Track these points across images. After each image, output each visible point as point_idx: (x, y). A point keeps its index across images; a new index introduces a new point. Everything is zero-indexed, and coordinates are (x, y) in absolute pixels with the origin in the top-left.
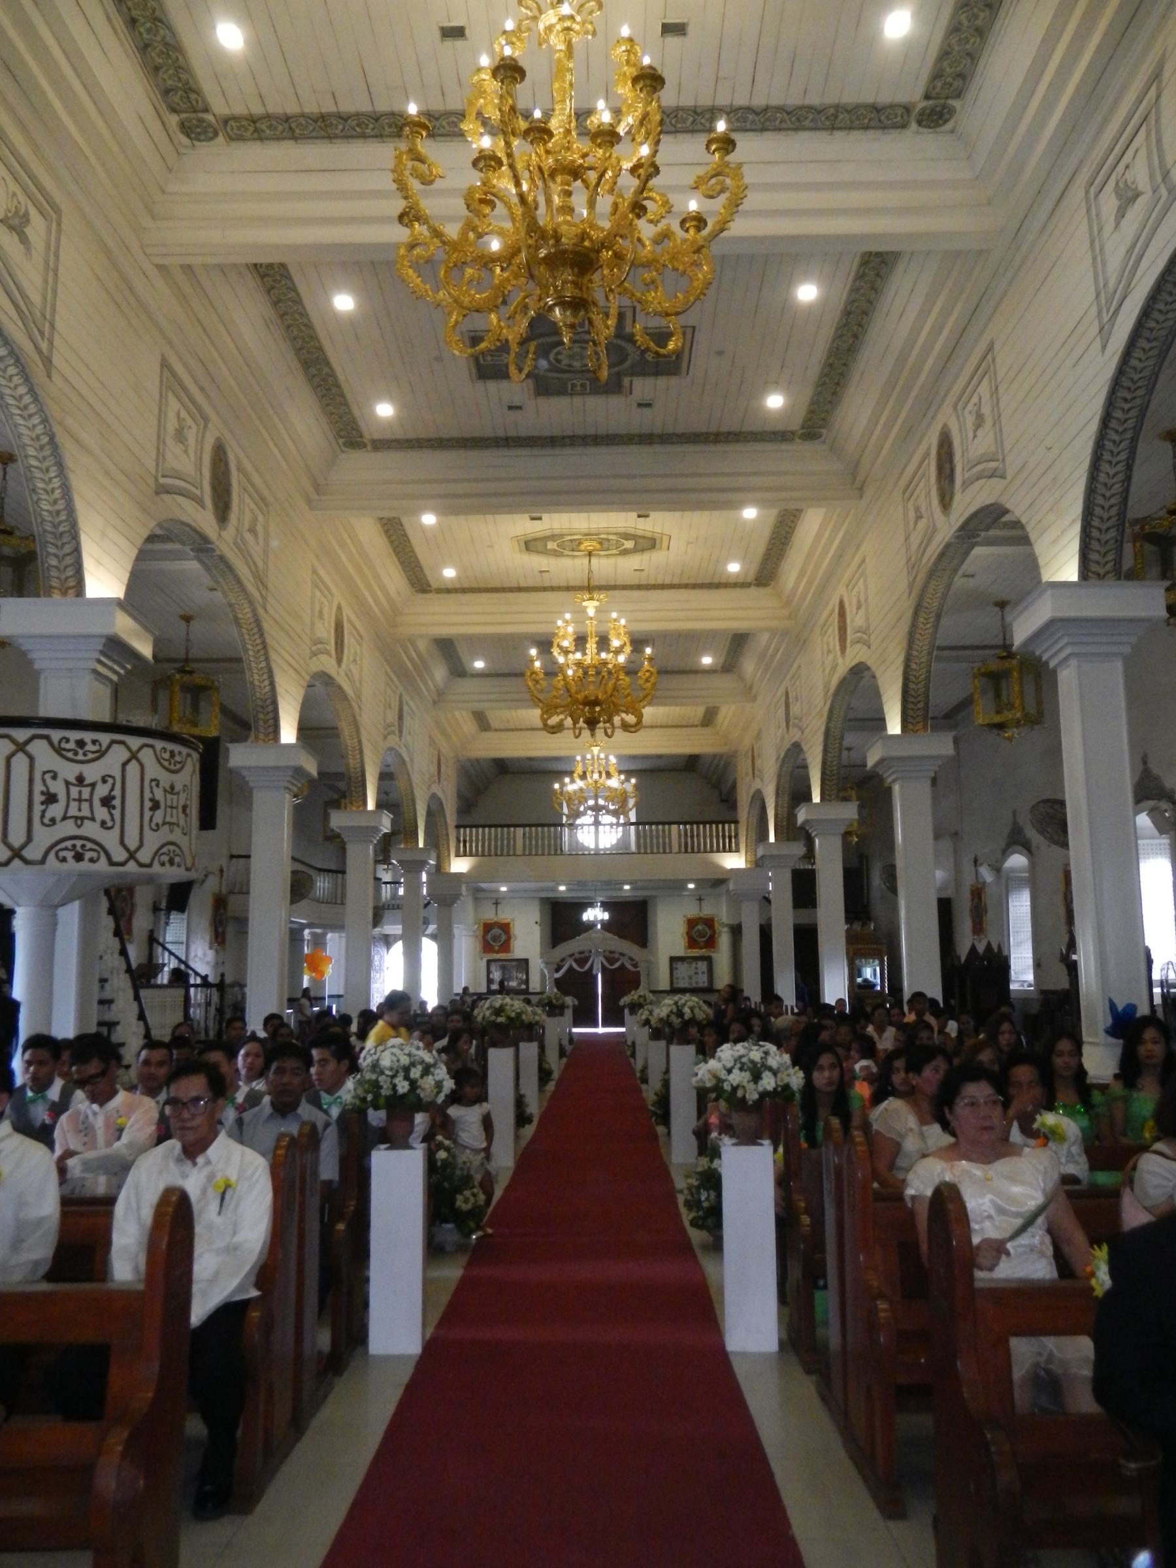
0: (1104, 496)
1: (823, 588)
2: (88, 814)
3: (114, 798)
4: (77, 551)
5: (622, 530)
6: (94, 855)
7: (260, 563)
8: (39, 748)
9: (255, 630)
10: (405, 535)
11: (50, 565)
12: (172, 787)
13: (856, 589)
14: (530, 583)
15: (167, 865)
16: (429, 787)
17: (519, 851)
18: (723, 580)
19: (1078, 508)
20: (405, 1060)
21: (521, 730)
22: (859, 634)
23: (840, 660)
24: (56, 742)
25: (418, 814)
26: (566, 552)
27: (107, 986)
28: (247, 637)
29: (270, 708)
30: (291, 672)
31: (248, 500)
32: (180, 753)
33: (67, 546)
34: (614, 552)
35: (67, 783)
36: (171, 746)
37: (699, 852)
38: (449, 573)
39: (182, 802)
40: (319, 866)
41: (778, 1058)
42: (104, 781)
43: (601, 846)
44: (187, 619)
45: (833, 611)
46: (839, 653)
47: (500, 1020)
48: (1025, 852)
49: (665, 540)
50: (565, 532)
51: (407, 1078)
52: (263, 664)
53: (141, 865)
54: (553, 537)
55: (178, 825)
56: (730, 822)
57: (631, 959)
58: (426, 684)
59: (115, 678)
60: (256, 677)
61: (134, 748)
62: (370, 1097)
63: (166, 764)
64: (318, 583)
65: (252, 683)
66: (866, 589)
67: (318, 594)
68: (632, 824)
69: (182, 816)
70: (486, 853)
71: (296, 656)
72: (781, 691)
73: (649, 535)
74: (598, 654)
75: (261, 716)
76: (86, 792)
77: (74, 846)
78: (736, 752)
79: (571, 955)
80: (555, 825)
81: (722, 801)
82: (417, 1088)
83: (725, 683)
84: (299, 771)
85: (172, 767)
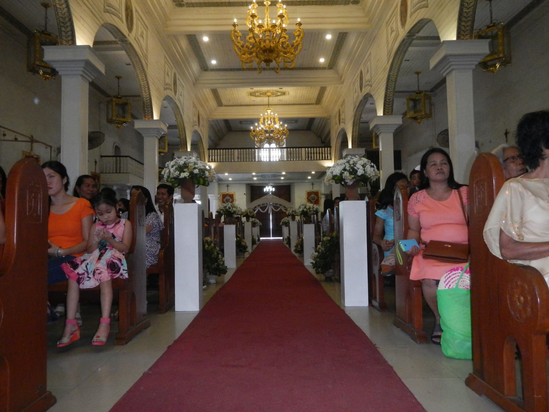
16: (193, 126)
21: (236, 106)
25: (187, 136)
29: (68, 24)
37: (314, 160)
45: (397, 6)
47: (183, 175)
56: (327, 147)
57: (284, 207)
58: (188, 70)
70: (222, 161)
72: (359, 72)
75: (63, 29)
78: (330, 116)
79: (259, 206)
80: (252, 148)
83: (329, 74)
84: (88, 64)
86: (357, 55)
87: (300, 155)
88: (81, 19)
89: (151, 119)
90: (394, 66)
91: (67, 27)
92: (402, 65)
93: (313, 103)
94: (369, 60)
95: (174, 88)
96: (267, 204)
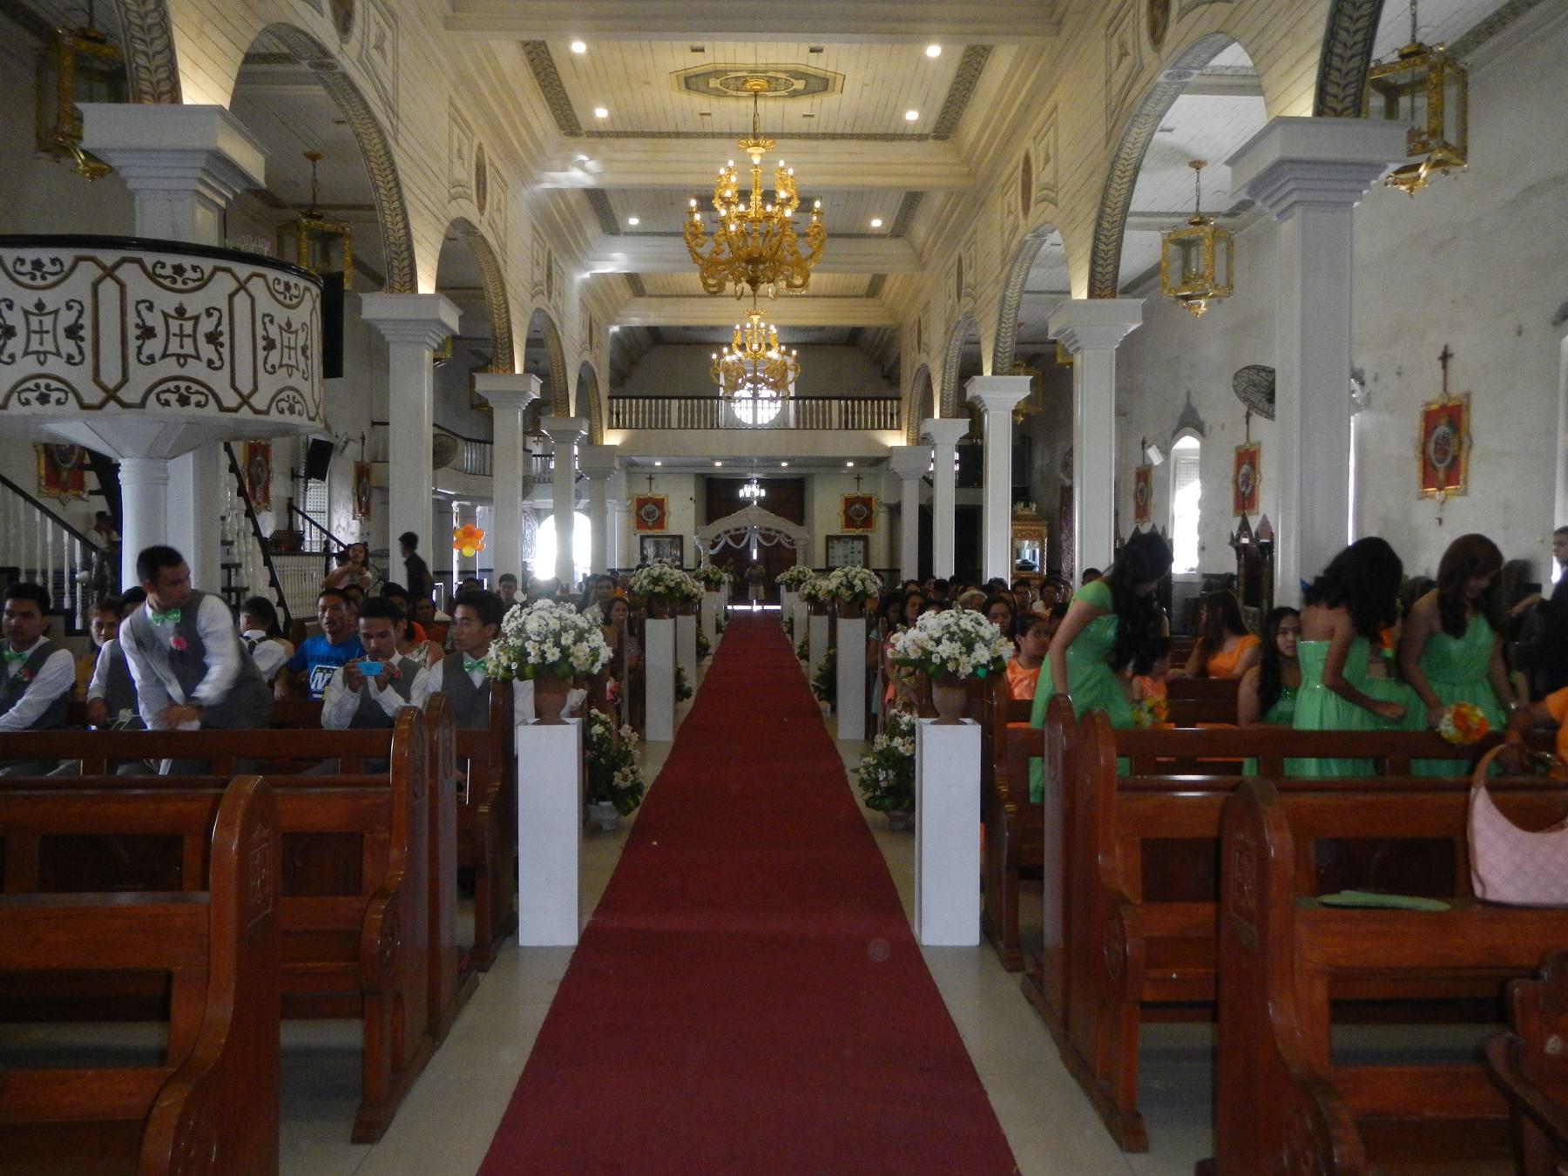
0: (1351, 18)
1: (1008, 141)
2: (194, 353)
3: (221, 334)
4: (169, 48)
5: (792, 67)
6: (202, 399)
7: (388, 86)
8: (129, 273)
9: (386, 165)
10: (553, 66)
11: (138, 65)
12: (289, 325)
13: (1045, 141)
14: (690, 128)
15: (287, 412)
17: (674, 424)
18: (900, 131)
19: (1320, 32)
20: (555, 625)
22: (1045, 192)
23: (1022, 222)
24: (150, 268)
26: (731, 92)
27: (235, 550)
28: (376, 171)
29: (406, 254)
30: (431, 219)
31: (373, 10)
32: (296, 285)
33: (158, 42)
34: (783, 93)
35: (166, 316)
36: (284, 277)
37: (859, 429)
38: (601, 113)
39: (301, 343)
40: (466, 436)
41: (990, 629)
42: (209, 314)
43: (759, 422)
44: (313, 157)
45: (1017, 167)
46: (1021, 215)
47: (658, 589)
48: (1198, 434)
49: (839, 77)
50: (729, 67)
51: (557, 644)
52: (396, 204)
53: (256, 412)
54: (716, 73)
55: (297, 369)
56: (892, 399)
57: (789, 537)
59: (222, 203)
60: (389, 218)
61: (243, 277)
62: (514, 666)
63: (281, 297)
64: (456, 117)
65: (384, 225)
66: (1056, 140)
67: (456, 129)
68: (791, 398)
69: (301, 359)
70: (640, 426)
71: (433, 198)
72: (955, 256)
73: (821, 73)
74: (764, 207)
75: (396, 263)
76: (188, 327)
77: (178, 388)
78: (901, 325)
80: (712, 398)
81: (886, 377)
82: (569, 656)
83: (895, 248)
85: (288, 301)
86: (950, 225)
87: (827, 417)
88: (424, 240)
89: (509, 372)
90: (1012, 279)
91: (402, 260)
92: (1030, 276)
93: (860, 294)
94: (973, 243)
95: (548, 286)
96: (746, 528)
